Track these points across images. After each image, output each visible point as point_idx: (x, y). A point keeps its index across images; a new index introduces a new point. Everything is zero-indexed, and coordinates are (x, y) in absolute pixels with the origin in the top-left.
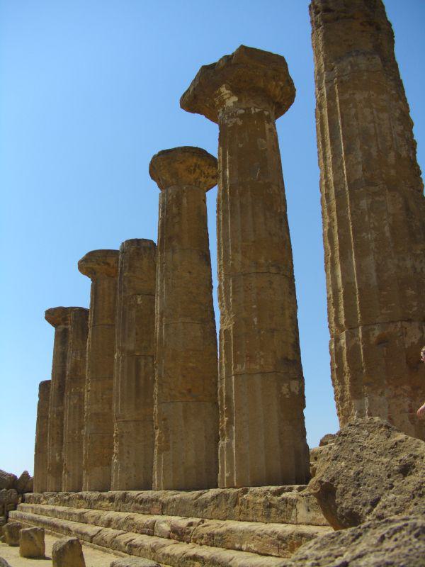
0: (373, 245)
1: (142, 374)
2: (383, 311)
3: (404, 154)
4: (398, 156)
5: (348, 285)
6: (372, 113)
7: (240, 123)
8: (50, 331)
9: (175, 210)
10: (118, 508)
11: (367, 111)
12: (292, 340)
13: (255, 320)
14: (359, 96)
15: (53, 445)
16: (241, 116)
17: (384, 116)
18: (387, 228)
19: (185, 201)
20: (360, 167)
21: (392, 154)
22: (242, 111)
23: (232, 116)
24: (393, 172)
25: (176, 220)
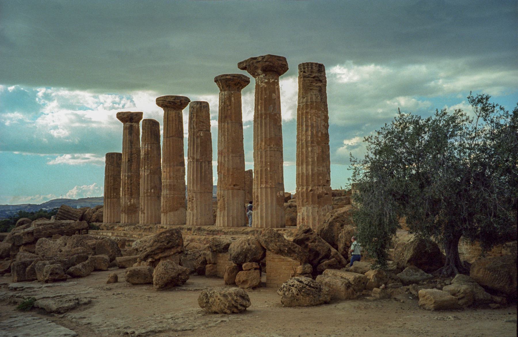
0: (311, 163)
1: (203, 171)
3: (324, 132)
4: (322, 133)
5: (303, 173)
7: (266, 86)
9: (228, 103)
10: (195, 234)
11: (314, 117)
12: (281, 176)
13: (269, 169)
14: (313, 111)
16: (266, 83)
17: (319, 119)
18: (316, 158)
19: (233, 99)
20: (310, 137)
21: (320, 133)
22: (266, 81)
24: (319, 139)
25: (229, 107)
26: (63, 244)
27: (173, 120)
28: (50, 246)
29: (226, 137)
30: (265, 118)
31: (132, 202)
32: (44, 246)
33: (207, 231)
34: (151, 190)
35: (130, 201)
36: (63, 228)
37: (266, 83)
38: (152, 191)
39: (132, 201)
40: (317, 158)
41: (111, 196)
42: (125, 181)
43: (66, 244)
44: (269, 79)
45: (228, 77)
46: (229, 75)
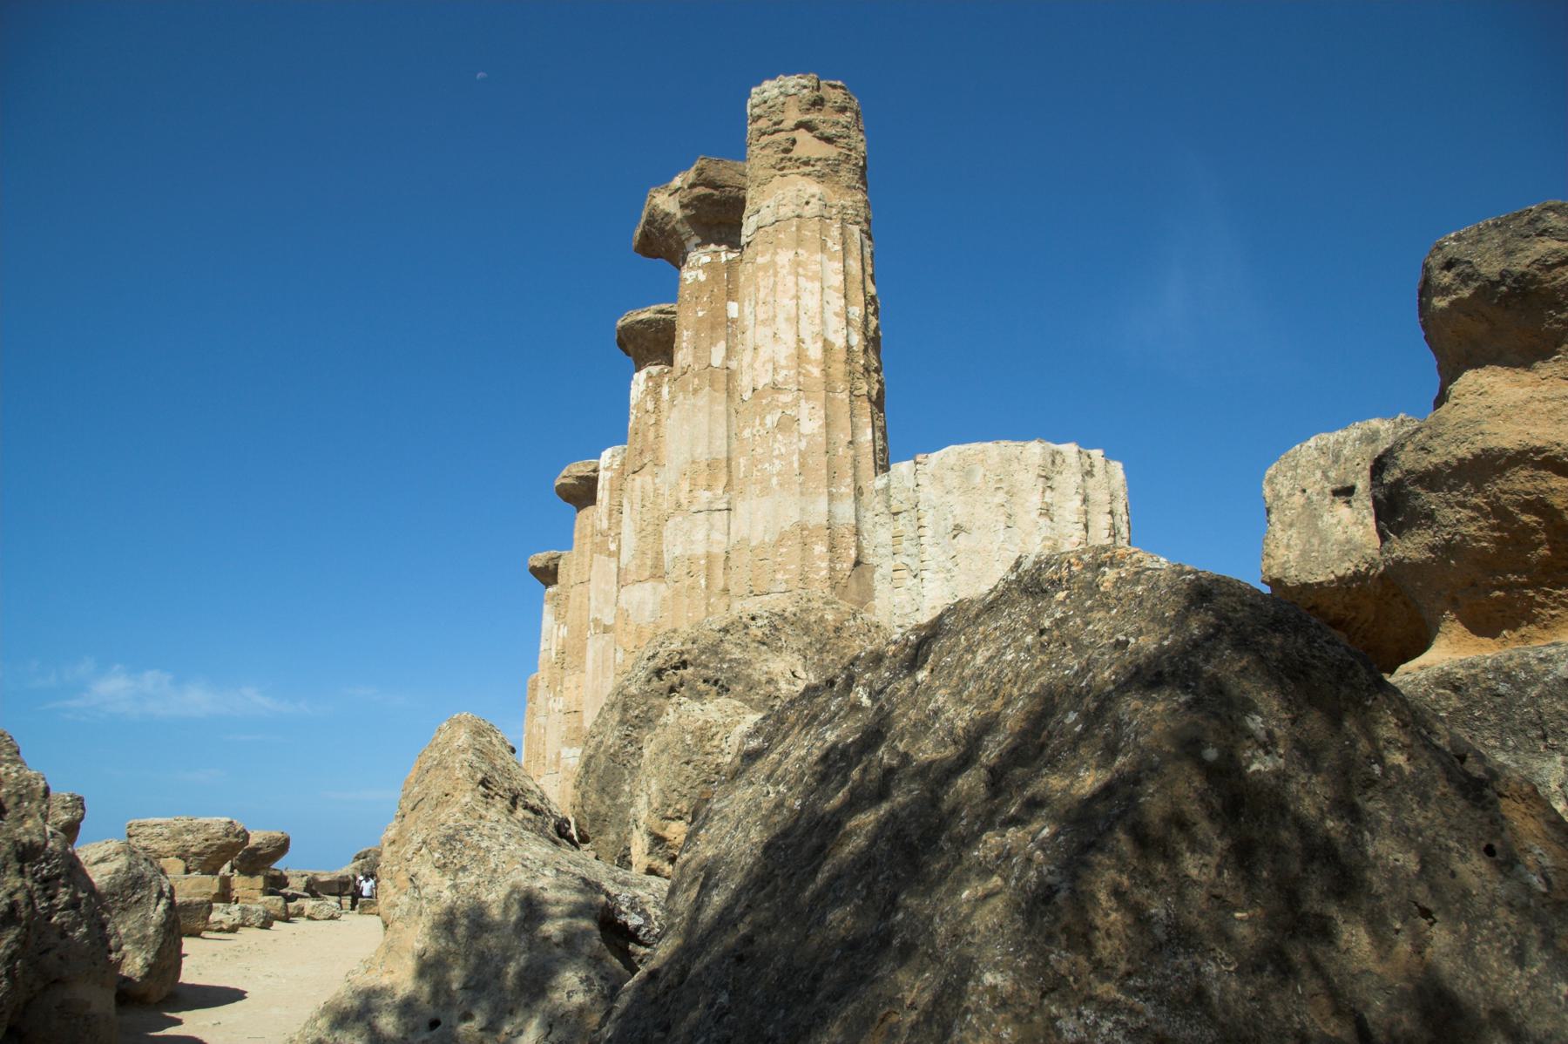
2: (779, 576)
6: (797, 284)
9: (650, 406)
13: (703, 582)
18: (795, 458)
19: (665, 390)
22: (707, 259)
37: (705, 267)
40: (802, 454)
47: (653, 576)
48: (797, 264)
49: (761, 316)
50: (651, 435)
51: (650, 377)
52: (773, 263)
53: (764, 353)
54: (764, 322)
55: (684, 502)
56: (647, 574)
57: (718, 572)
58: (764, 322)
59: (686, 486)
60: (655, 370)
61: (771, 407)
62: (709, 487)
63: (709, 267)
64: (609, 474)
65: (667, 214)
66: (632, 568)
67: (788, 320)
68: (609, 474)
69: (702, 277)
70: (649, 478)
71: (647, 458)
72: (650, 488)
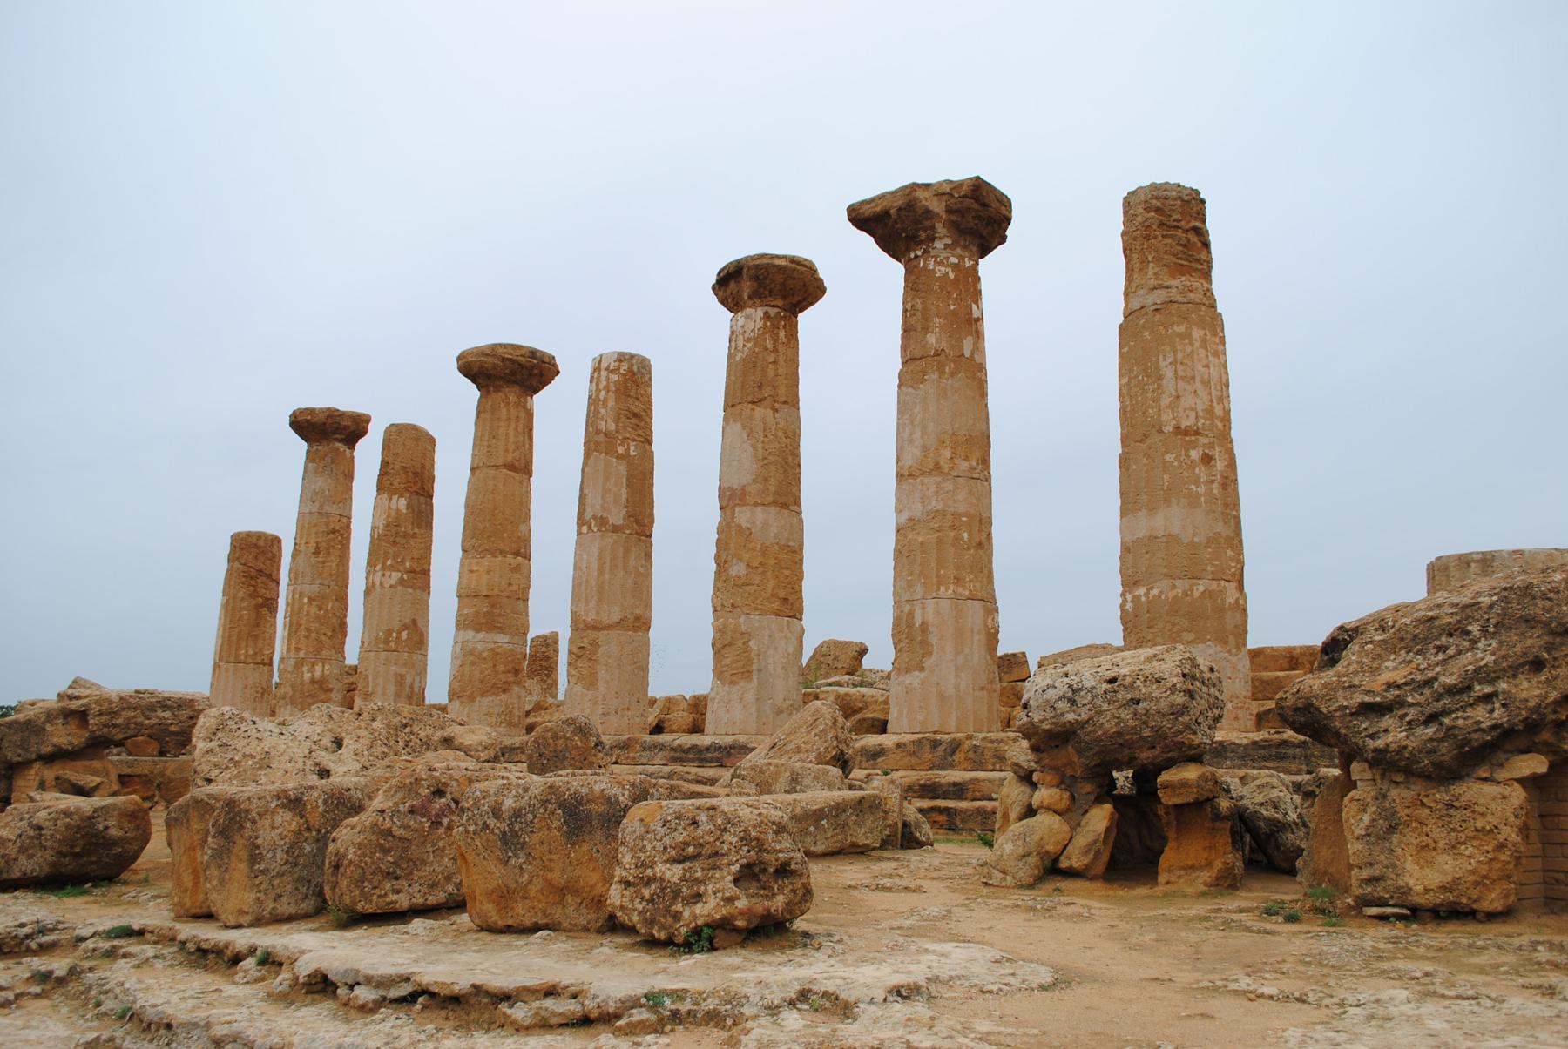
8: (301, 446)
9: (769, 344)
13: (965, 535)
15: (298, 649)
22: (954, 260)
23: (940, 263)
26: (327, 741)
27: (509, 419)
28: (266, 745)
29: (760, 446)
30: (952, 374)
31: (318, 674)
32: (240, 744)
33: (673, 749)
34: (399, 632)
35: (312, 670)
36: (167, 714)
37: (955, 267)
38: (404, 635)
39: (318, 668)
41: (237, 656)
42: (301, 608)
43: (338, 743)
44: (961, 258)
45: (777, 262)
46: (784, 257)
47: (775, 503)
48: (1204, 341)
49: (1181, 373)
50: (771, 372)
51: (767, 316)
52: (1187, 335)
53: (1188, 400)
54: (1183, 378)
55: (946, 467)
56: (770, 499)
57: (976, 530)
58: (1183, 378)
59: (947, 453)
60: (773, 311)
61: (1193, 445)
62: (966, 459)
63: (955, 267)
64: (616, 378)
65: (928, 211)
66: (752, 489)
67: (1202, 382)
68: (616, 378)
69: (952, 275)
70: (770, 412)
71: (767, 391)
72: (771, 420)
